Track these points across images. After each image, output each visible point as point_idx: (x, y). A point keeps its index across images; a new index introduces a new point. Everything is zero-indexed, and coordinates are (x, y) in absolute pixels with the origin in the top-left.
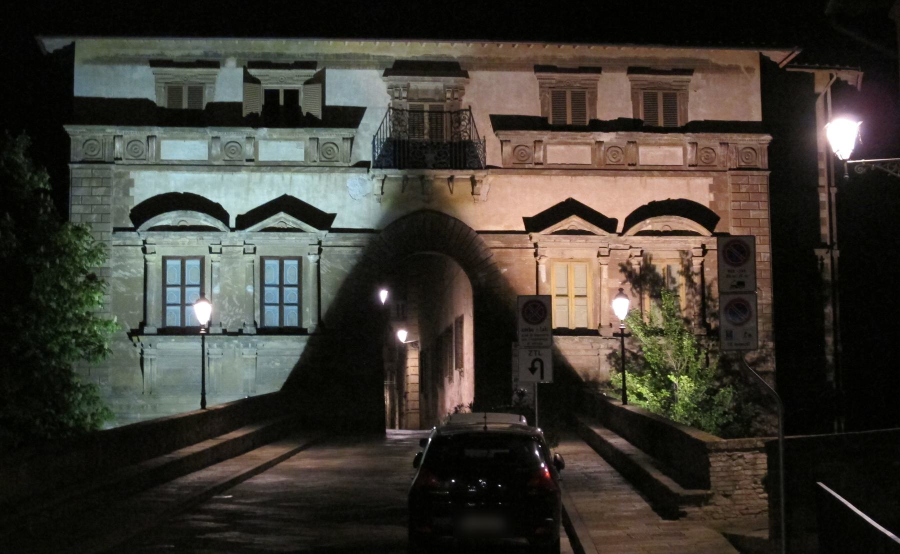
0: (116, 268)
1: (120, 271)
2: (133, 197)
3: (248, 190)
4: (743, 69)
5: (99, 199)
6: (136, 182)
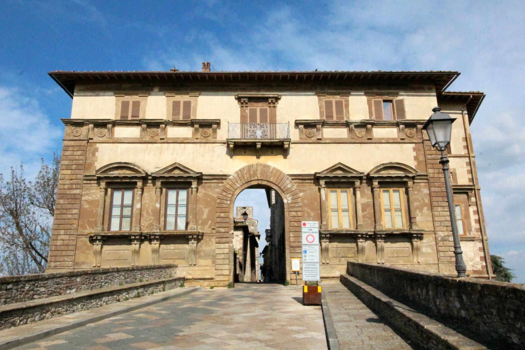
1: (86, 196)
2: (97, 157)
4: (426, 88)
5: (77, 157)
6: (99, 149)
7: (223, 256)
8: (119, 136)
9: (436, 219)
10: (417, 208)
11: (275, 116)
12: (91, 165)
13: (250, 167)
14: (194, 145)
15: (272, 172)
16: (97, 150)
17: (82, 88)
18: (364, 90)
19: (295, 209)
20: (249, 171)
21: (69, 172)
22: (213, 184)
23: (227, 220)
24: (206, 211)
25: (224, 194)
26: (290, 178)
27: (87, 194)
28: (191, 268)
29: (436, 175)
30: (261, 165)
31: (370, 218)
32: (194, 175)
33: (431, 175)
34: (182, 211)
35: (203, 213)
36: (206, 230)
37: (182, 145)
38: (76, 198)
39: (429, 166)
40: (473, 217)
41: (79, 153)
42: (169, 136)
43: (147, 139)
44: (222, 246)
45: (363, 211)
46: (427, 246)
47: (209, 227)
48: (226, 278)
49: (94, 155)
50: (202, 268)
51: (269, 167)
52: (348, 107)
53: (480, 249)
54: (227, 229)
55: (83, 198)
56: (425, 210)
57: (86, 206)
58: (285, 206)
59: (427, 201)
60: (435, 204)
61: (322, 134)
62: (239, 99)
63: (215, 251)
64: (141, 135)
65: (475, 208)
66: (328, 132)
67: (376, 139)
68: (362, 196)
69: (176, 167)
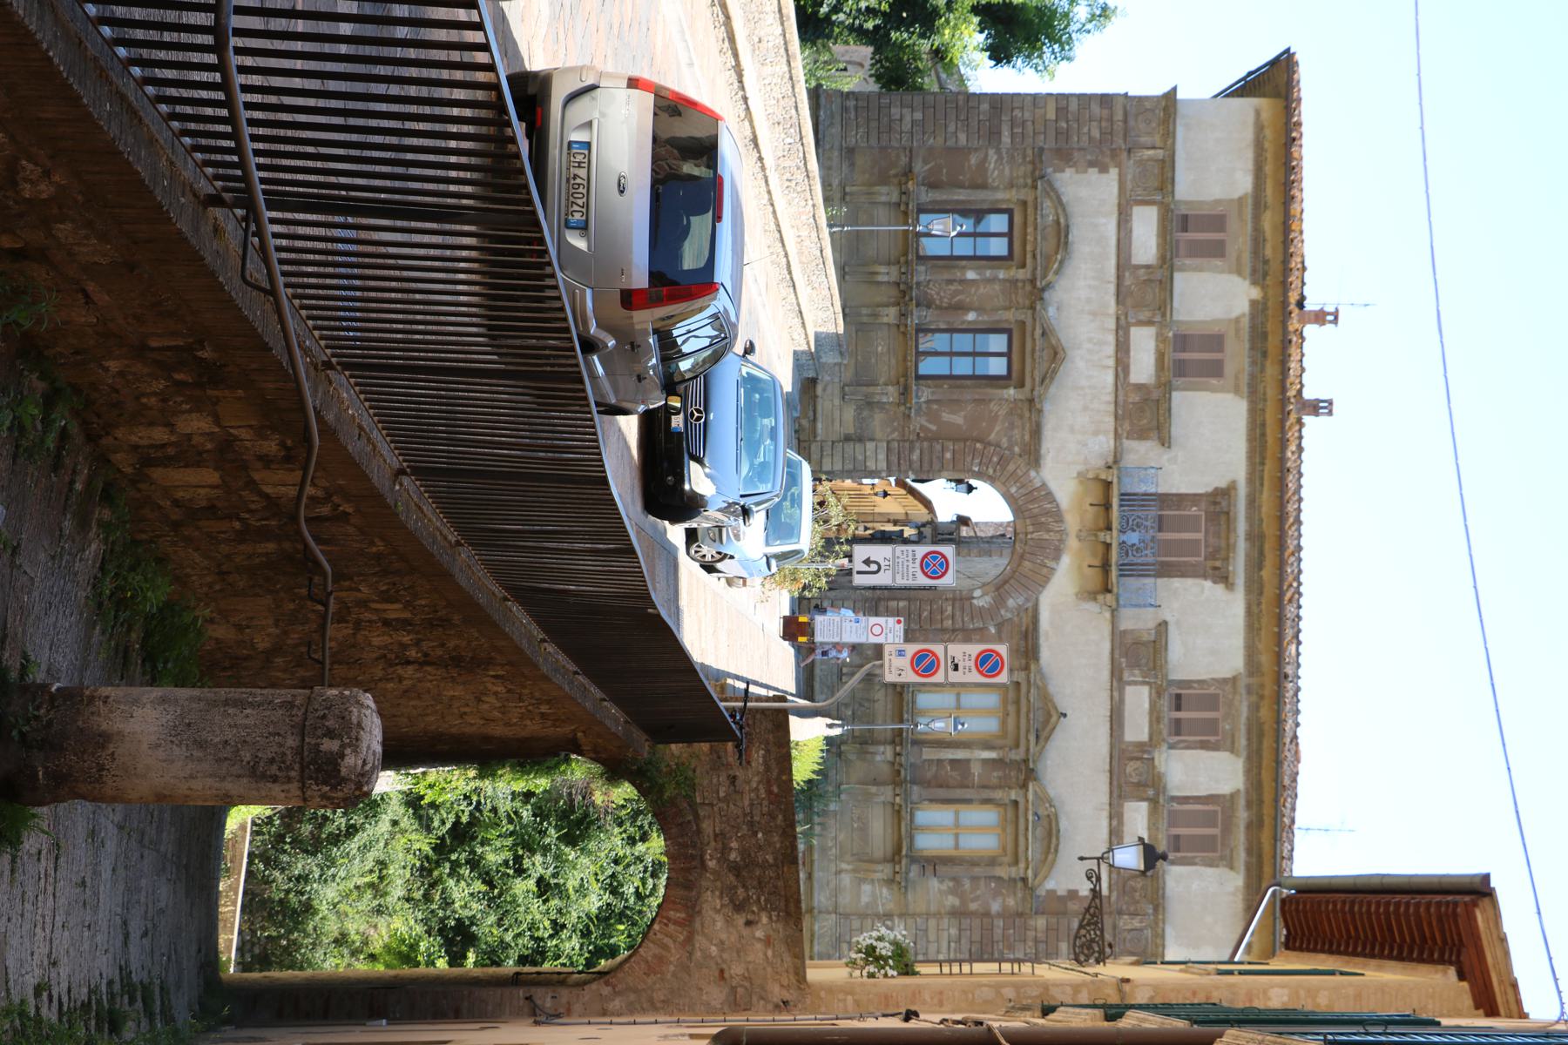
3: (1094, 314)
6: (1104, 176)
7: (860, 457)
8: (1134, 217)
9: (932, 923)
11: (1183, 575)
13: (1058, 515)
16: (1104, 169)
17: (1265, 116)
18: (1247, 792)
19: (958, 613)
20: (1047, 513)
21: (1051, 115)
24: (957, 419)
26: (1030, 605)
27: (1000, 158)
28: (837, 392)
29: (1031, 934)
30: (1061, 541)
33: (1032, 923)
34: (963, 367)
35: (952, 412)
36: (919, 422)
37: (1111, 362)
41: (1096, 134)
42: (1133, 330)
44: (882, 456)
45: (952, 761)
46: (873, 894)
49: (1091, 164)
50: (837, 414)
51: (1057, 558)
52: (1202, 748)
54: (916, 465)
56: (952, 901)
59: (973, 906)
60: (966, 922)
61: (1135, 683)
63: (872, 440)
67: (1122, 806)
68: (985, 761)
69: (1056, 355)
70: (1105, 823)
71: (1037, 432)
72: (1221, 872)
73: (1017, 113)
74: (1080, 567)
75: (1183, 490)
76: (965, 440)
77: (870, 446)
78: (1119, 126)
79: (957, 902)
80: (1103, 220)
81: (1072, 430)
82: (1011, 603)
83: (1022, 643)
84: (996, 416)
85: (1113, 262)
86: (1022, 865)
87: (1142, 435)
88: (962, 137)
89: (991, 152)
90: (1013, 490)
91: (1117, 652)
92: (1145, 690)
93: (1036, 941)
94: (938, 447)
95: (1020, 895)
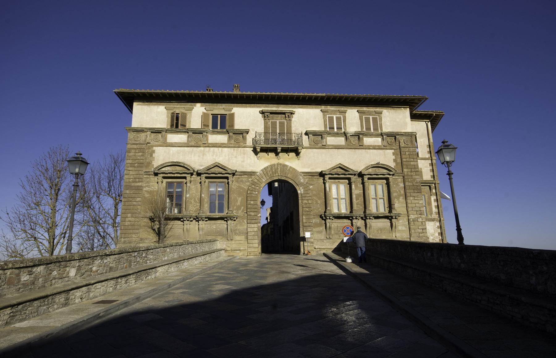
0: (145, 187)
3: (204, 154)
5: (139, 157)
7: (253, 233)
8: (171, 142)
10: (396, 197)
11: (291, 127)
12: (149, 164)
13: (272, 166)
14: (229, 149)
15: (289, 170)
16: (154, 152)
19: (307, 198)
22: (244, 178)
23: (255, 206)
24: (240, 199)
25: (253, 186)
27: (147, 186)
28: (230, 242)
29: (409, 173)
30: (280, 164)
31: (361, 205)
32: (230, 172)
33: (406, 173)
35: (237, 201)
36: (240, 213)
37: (220, 149)
38: (139, 188)
39: (404, 166)
40: (434, 204)
41: (140, 154)
42: (209, 142)
43: (193, 144)
44: (253, 225)
45: (356, 200)
47: (242, 211)
48: (256, 250)
49: (151, 155)
51: (287, 166)
53: (438, 227)
55: (145, 189)
56: (402, 199)
57: (147, 195)
58: (299, 196)
60: (408, 194)
62: (262, 113)
64: (188, 140)
65: (435, 197)
66: (330, 140)
68: (356, 189)
70: (371, 151)
71: (244, 173)
72: (383, 115)
73: (131, 180)
74: (289, 159)
75: (263, 127)
76: (247, 197)
77: (249, 230)
78: (138, 146)
79: (402, 197)
80: (171, 152)
81: (243, 161)
82: (302, 181)
83: (315, 177)
84: (238, 186)
85: (186, 148)
86: (388, 176)
87: (244, 138)
88: (138, 199)
89: (145, 189)
90: (264, 180)
91: (316, 147)
92: (328, 138)
93: (411, 172)
94: (249, 206)
95: (397, 177)
